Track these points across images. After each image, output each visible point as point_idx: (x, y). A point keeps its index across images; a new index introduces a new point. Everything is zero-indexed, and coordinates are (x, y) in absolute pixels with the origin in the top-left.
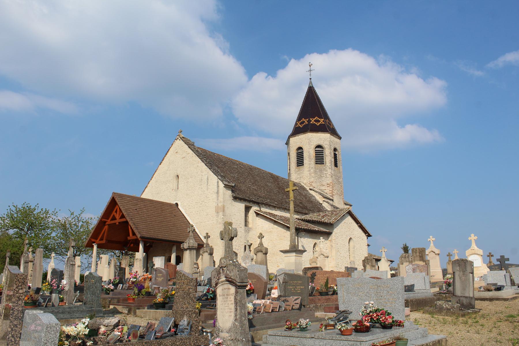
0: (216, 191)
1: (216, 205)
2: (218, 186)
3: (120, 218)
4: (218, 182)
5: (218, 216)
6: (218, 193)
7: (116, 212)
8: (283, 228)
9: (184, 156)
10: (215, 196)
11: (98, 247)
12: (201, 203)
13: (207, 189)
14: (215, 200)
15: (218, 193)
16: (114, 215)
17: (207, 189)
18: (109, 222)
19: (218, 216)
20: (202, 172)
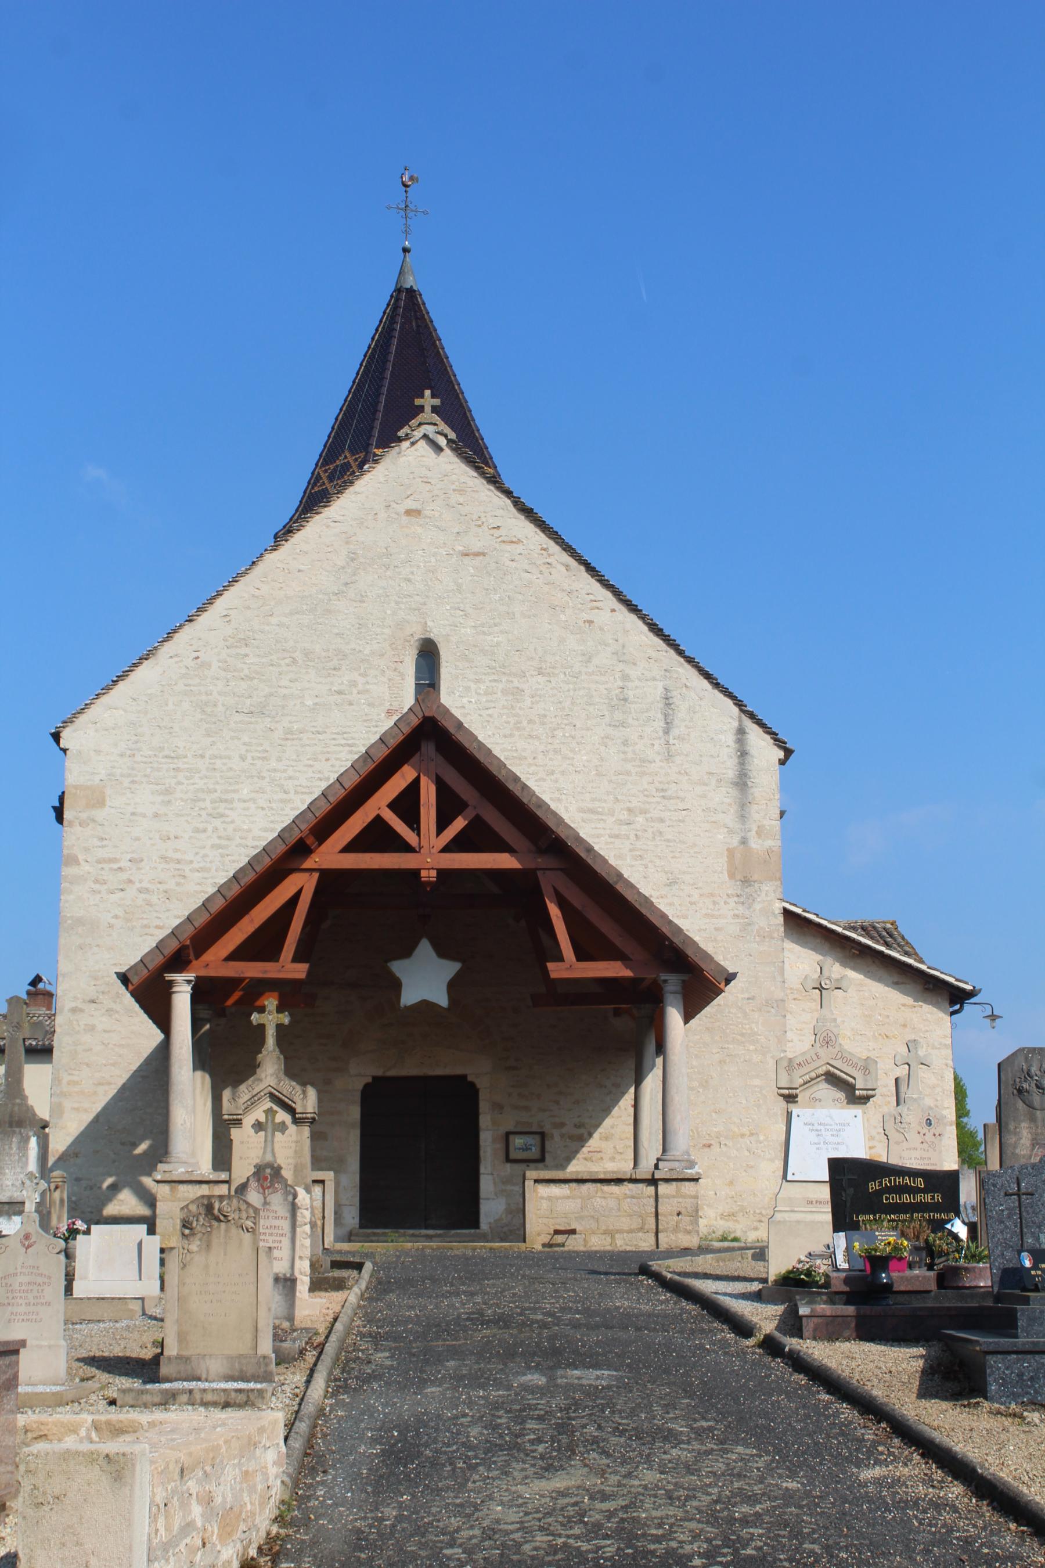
0: (731, 774)
1: (735, 841)
2: (743, 754)
3: (445, 849)
4: (741, 731)
5: (747, 901)
6: (742, 782)
7: (407, 805)
8: (895, 985)
9: (477, 546)
10: (724, 797)
11: (196, 999)
12: (624, 816)
13: (669, 757)
14: (730, 818)
15: (742, 782)
16: (378, 820)
17: (669, 757)
18: (330, 855)
19: (747, 901)
20: (620, 656)
